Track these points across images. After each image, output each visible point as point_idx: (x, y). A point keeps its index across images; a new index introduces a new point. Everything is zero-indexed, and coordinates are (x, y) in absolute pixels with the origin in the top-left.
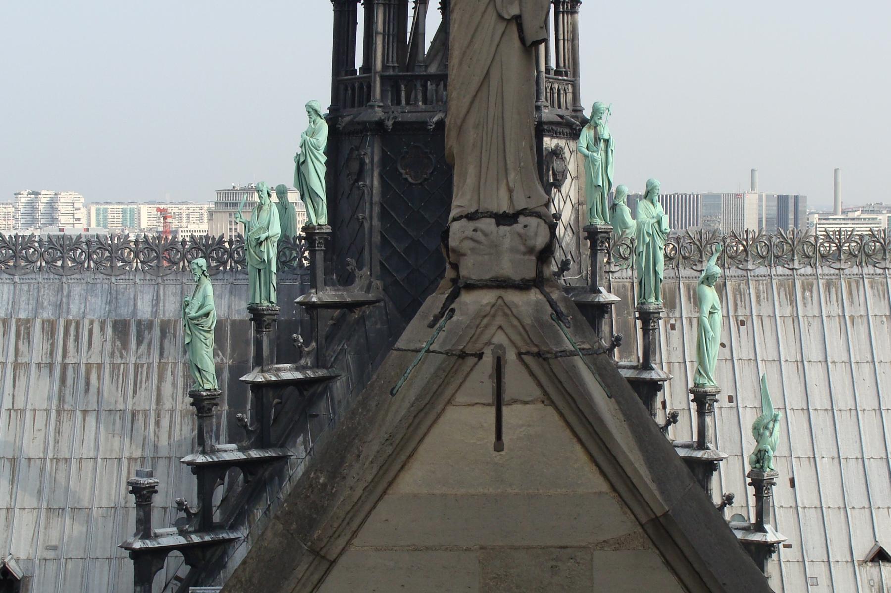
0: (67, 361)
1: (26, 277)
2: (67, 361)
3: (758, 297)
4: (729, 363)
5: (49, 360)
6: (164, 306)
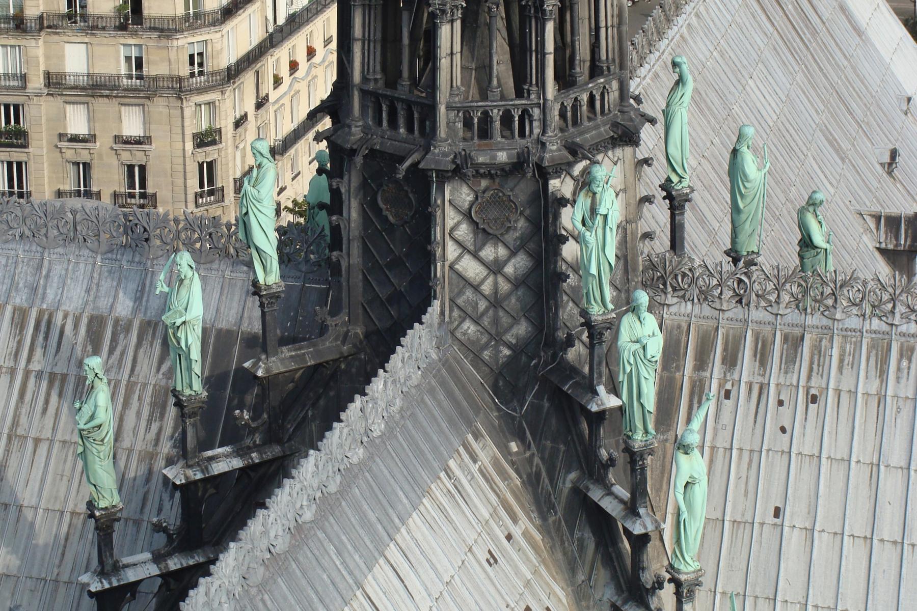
0: (31, 367)
1: (7, 246)
2: (31, 367)
3: (841, 361)
4: (785, 457)
5: (12, 364)
6: (148, 301)
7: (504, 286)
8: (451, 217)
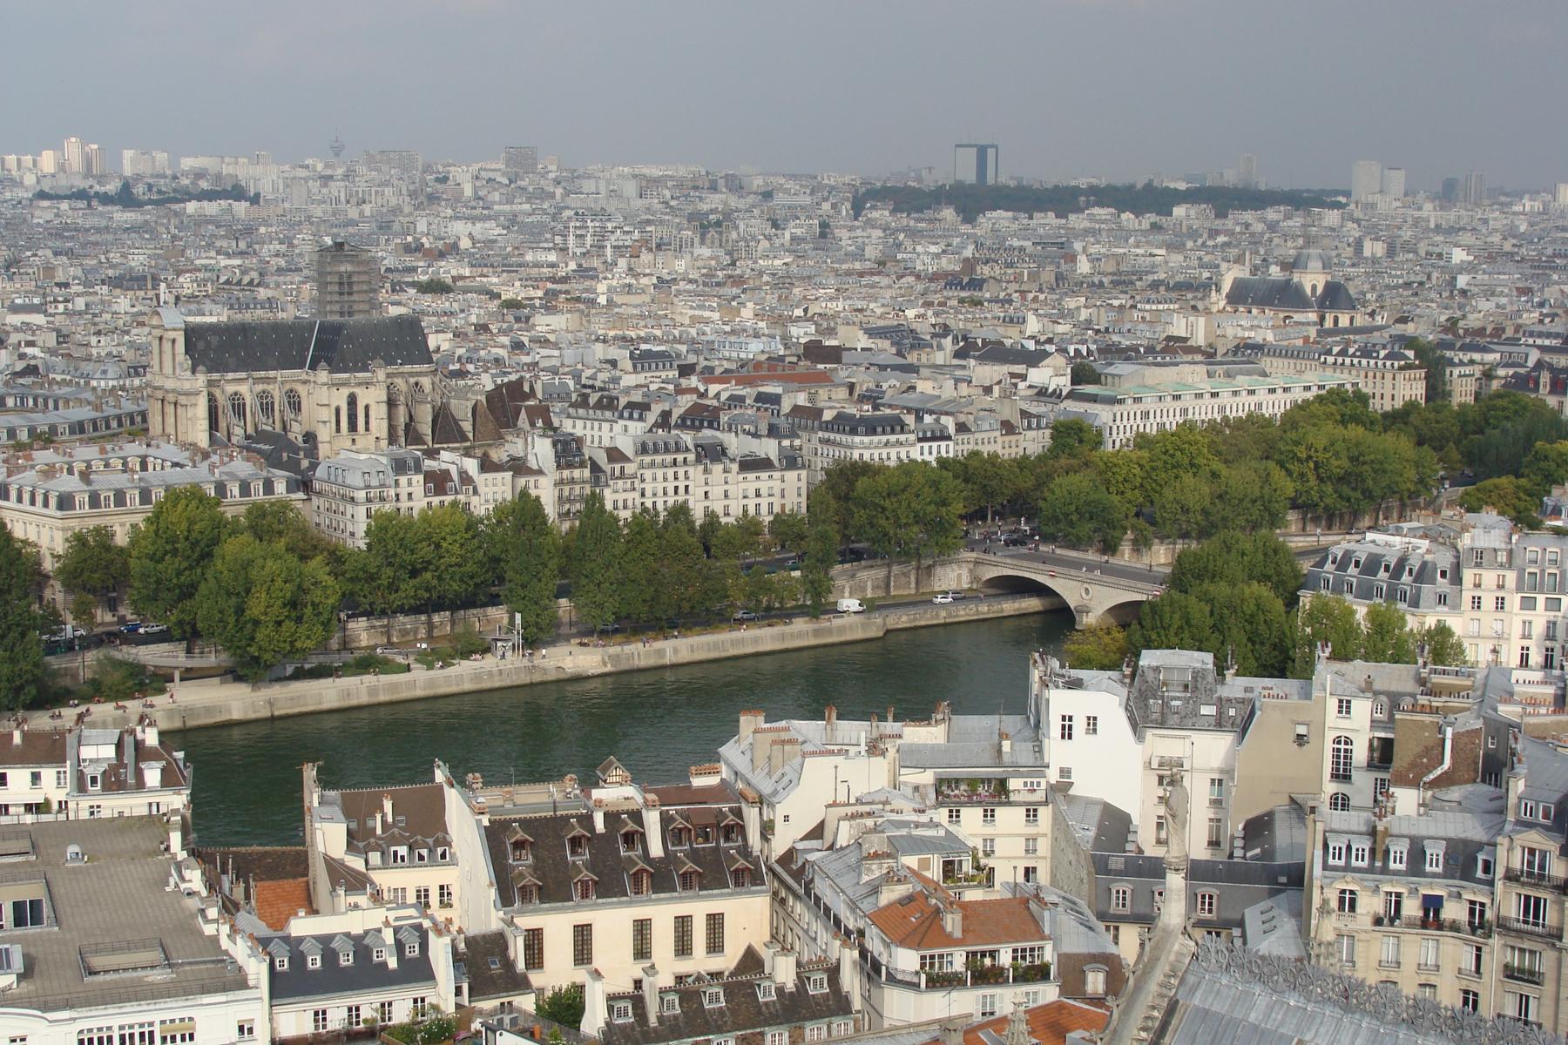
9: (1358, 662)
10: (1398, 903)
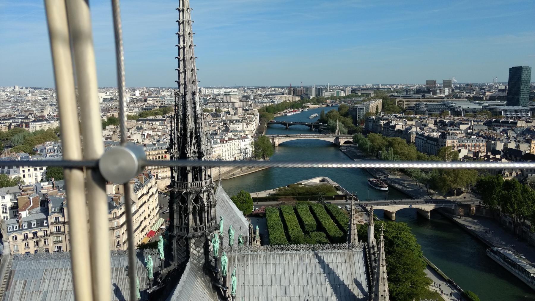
7: (200, 254)
8: (192, 244)
9: (4, 188)
10: (27, 236)
